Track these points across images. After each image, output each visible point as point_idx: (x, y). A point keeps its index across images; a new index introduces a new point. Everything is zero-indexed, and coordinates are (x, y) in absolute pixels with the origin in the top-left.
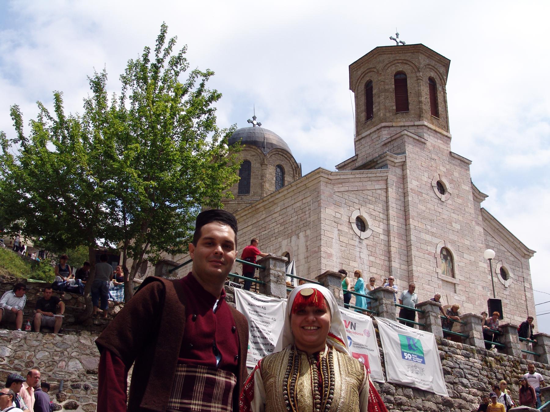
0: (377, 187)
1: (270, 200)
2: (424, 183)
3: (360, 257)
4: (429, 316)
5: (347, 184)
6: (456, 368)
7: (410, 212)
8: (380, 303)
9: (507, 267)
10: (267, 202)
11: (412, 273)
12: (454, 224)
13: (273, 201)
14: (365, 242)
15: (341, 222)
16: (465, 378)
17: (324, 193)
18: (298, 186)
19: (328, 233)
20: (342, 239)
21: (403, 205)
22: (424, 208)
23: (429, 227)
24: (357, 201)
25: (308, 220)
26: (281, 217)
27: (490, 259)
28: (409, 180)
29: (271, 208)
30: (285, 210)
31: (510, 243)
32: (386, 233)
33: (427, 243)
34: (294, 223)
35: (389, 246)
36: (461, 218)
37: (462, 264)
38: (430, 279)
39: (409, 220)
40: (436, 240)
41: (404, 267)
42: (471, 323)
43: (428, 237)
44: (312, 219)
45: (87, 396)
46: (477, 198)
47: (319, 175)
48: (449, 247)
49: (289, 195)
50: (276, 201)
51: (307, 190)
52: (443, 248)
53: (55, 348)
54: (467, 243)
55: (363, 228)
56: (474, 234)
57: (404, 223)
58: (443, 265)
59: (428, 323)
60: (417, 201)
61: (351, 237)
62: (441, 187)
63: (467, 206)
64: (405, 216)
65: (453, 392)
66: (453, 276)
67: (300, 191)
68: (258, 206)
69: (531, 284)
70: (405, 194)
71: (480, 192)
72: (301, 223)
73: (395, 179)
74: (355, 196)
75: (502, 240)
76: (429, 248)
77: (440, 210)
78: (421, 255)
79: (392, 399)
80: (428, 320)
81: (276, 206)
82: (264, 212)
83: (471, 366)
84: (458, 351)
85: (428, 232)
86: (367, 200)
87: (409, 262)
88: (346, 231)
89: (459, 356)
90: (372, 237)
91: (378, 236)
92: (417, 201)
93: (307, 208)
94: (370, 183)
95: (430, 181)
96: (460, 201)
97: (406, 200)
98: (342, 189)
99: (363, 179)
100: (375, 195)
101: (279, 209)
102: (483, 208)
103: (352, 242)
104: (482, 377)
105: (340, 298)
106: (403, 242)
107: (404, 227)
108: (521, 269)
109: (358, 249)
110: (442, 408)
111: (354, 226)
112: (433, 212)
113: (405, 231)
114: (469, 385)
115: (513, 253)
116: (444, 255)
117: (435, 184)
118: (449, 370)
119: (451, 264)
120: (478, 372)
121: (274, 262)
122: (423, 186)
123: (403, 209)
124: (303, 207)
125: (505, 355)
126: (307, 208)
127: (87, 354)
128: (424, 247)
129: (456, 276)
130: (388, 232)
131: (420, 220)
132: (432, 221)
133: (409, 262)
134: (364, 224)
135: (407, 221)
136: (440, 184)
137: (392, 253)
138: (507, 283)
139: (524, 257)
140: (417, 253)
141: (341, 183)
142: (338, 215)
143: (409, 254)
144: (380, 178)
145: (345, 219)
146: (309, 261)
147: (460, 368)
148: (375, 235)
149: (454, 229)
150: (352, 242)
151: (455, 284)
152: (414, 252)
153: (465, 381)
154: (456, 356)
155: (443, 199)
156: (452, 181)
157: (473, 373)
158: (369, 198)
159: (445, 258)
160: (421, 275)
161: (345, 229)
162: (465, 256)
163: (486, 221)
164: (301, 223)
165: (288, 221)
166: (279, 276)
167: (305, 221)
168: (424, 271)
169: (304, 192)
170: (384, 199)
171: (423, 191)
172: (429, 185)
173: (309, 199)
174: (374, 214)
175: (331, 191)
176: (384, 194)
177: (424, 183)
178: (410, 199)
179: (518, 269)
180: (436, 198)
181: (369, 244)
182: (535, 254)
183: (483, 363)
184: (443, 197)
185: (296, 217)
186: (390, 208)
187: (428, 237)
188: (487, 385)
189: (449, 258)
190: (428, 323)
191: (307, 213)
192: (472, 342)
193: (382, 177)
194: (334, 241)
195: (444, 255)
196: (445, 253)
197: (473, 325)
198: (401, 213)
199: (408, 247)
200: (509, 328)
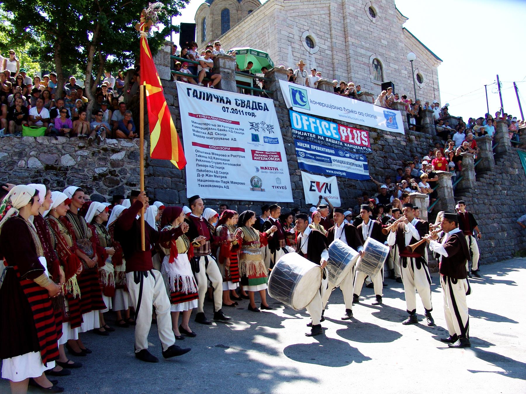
0: (322, 12)
1: (239, 30)
2: (359, 8)
3: (310, 68)
5: (298, 10)
6: (385, 146)
7: (349, 31)
9: (422, 73)
10: (237, 32)
12: (383, 41)
13: (241, 30)
14: (313, 56)
15: (293, 41)
17: (278, 18)
18: (258, 15)
19: (284, 50)
20: (295, 54)
21: (343, 26)
22: (359, 29)
23: (363, 43)
24: (306, 24)
25: (268, 41)
26: (247, 42)
27: (412, 61)
28: (347, 6)
29: (240, 36)
30: (250, 36)
31: (423, 54)
32: (331, 49)
33: (362, 55)
34: (257, 46)
35: (333, 59)
36: (388, 36)
37: (389, 71)
38: (365, 83)
39: (348, 39)
40: (369, 54)
41: (344, 75)
43: (363, 51)
44: (270, 40)
46: (399, 20)
47: (274, 4)
48: (379, 58)
49: (252, 24)
50: (243, 30)
51: (266, 17)
52: (375, 59)
53: (14, 149)
54: (393, 55)
55: (312, 46)
56: (398, 48)
57: (344, 41)
58: (374, 72)
60: (354, 23)
61: (302, 52)
62: (372, 12)
63: (393, 27)
64: (345, 35)
67: (260, 19)
68: (230, 36)
69: (438, 86)
70: (344, 18)
71: (402, 15)
72: (263, 44)
73: (336, 5)
74: (304, 20)
75: (418, 53)
76: (364, 59)
77: (372, 30)
78: (358, 64)
81: (243, 34)
82: (235, 40)
85: (362, 47)
86: (314, 23)
87: (349, 71)
88: (298, 48)
90: (319, 52)
91: (324, 52)
92: (354, 23)
93: (267, 32)
94: (316, 9)
95: (363, 6)
96: (387, 23)
97: (345, 22)
98: (294, 15)
99: (310, 6)
100: (321, 19)
101: (246, 36)
102: (404, 28)
103: (304, 57)
106: (343, 56)
107: (344, 43)
108: (431, 75)
109: (308, 62)
111: (305, 43)
112: (367, 31)
113: (345, 47)
115: (426, 63)
116: (375, 65)
117: (367, 9)
119: (381, 71)
120: (403, 148)
121: (223, 61)
122: (358, 11)
123: (343, 29)
124: (263, 32)
125: (424, 134)
126: (267, 32)
127: (45, 153)
128: (360, 59)
130: (332, 49)
131: (356, 38)
132: (366, 38)
133: (348, 72)
134: (313, 42)
135: (347, 39)
136: (372, 9)
137: (335, 64)
138: (422, 85)
139: (433, 66)
140: (354, 63)
141: (293, 10)
142: (291, 36)
143: (349, 64)
144: (324, 5)
145: (297, 37)
147: (389, 145)
148: (321, 51)
149: (382, 45)
150: (304, 57)
152: (352, 63)
153: (392, 155)
154: (386, 136)
155: (374, 21)
156: (381, 7)
158: (316, 21)
159: (376, 67)
160: (358, 80)
161: (297, 46)
162: (391, 65)
163: (407, 39)
164: (263, 44)
165: (253, 45)
166: (228, 73)
167: (266, 42)
168: (360, 77)
169: (263, 19)
170: (328, 21)
171: (358, 15)
172: (363, 10)
173: (267, 24)
174: (320, 34)
175: (284, 16)
176: (328, 18)
177: (359, 8)
178: (348, 21)
179: (429, 75)
180: (369, 20)
181: (317, 58)
182: (442, 63)
184: (374, 20)
185: (259, 40)
186: (333, 29)
187: (363, 51)
188: (410, 157)
189: (379, 67)
191: (267, 35)
193: (325, 4)
194: (289, 56)
195: (375, 65)
196: (376, 63)
198: (342, 33)
199: (348, 59)
200: (427, 113)
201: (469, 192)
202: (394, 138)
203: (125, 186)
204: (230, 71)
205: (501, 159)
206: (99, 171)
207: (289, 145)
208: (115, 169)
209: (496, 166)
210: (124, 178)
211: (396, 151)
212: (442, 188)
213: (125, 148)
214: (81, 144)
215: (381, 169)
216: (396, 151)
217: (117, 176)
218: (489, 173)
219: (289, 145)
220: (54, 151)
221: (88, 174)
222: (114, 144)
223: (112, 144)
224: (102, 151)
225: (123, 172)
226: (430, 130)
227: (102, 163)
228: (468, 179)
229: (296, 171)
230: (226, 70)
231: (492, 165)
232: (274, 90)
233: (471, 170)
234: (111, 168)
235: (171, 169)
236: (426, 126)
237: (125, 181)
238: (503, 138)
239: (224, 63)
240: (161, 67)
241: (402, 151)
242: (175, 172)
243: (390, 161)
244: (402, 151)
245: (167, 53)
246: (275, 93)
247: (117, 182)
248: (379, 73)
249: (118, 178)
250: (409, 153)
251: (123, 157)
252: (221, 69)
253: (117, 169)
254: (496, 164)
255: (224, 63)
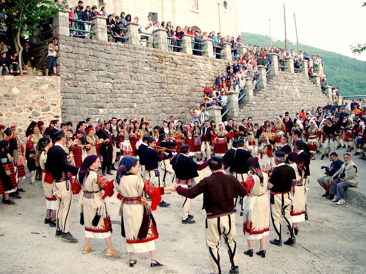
4: (185, 42)
8: (159, 38)
11: (175, 8)
16: (203, 75)
42: (207, 44)
45: (7, 109)
59: (185, 46)
65: (197, 83)
66: (198, 9)
79: (166, 91)
80: (185, 45)
83: (206, 68)
84: (200, 61)
89: (200, 64)
104: (211, 73)
105: (137, 37)
110: (191, 93)
114: (205, 79)
118: (195, 71)
121: (100, 20)
125: (224, 60)
129: (199, 8)
146: (115, 4)
151: (198, 13)
153: (202, 77)
154: (199, 63)
157: (207, 72)
166: (103, 28)
183: (212, 65)
188: (214, 78)
190: (185, 46)
192: (207, 55)
197: (208, 45)
201: (248, 103)
202: (204, 64)
203: (51, 106)
204: (104, 27)
205: (271, 80)
206: (35, 96)
207: (139, 74)
208: (43, 95)
209: (268, 85)
210: (49, 101)
211: (204, 74)
212: (232, 102)
213: (48, 82)
214: (22, 81)
215: (195, 87)
216: (204, 74)
217: (45, 100)
218: (262, 90)
219: (139, 74)
220: (7, 85)
221: (28, 99)
222: (41, 80)
223: (40, 80)
224: (34, 84)
225: (49, 97)
226: (228, 57)
227: (35, 92)
228: (249, 96)
229: (144, 91)
230: (101, 26)
231: (265, 84)
232: (130, 37)
233: (251, 89)
234: (41, 95)
235: (75, 94)
236: (226, 55)
237: (50, 103)
238: (274, 65)
239: (100, 21)
240: (64, 28)
241: (208, 74)
242: (76, 96)
243: (200, 80)
244: (208, 74)
245: (67, 17)
246: (130, 39)
247: (46, 104)
248: (196, 3)
249: (46, 101)
250: (213, 75)
251: (47, 87)
252: (98, 26)
253: (45, 96)
254: (268, 84)
255: (100, 21)
